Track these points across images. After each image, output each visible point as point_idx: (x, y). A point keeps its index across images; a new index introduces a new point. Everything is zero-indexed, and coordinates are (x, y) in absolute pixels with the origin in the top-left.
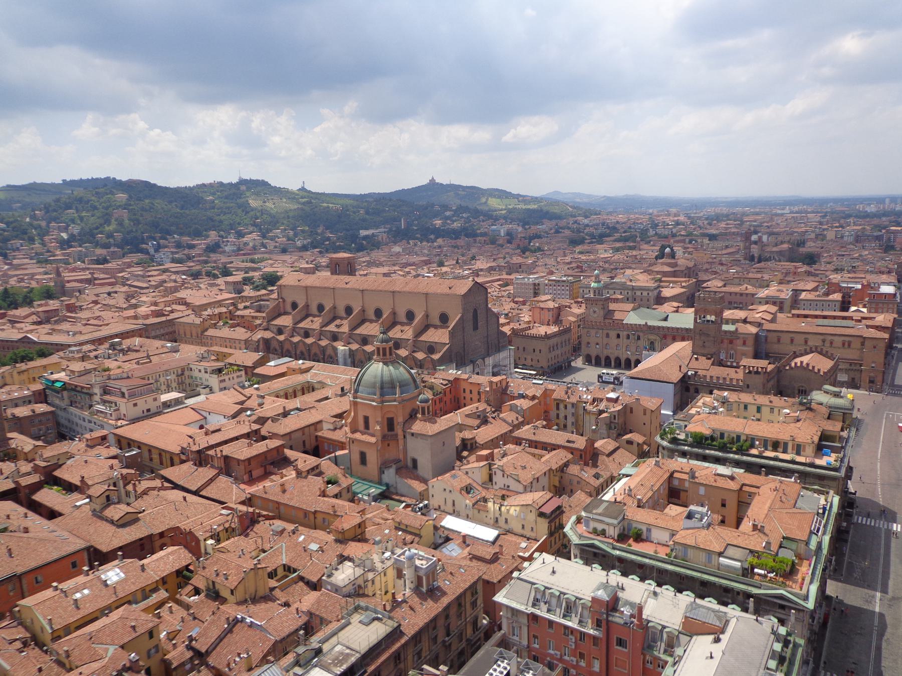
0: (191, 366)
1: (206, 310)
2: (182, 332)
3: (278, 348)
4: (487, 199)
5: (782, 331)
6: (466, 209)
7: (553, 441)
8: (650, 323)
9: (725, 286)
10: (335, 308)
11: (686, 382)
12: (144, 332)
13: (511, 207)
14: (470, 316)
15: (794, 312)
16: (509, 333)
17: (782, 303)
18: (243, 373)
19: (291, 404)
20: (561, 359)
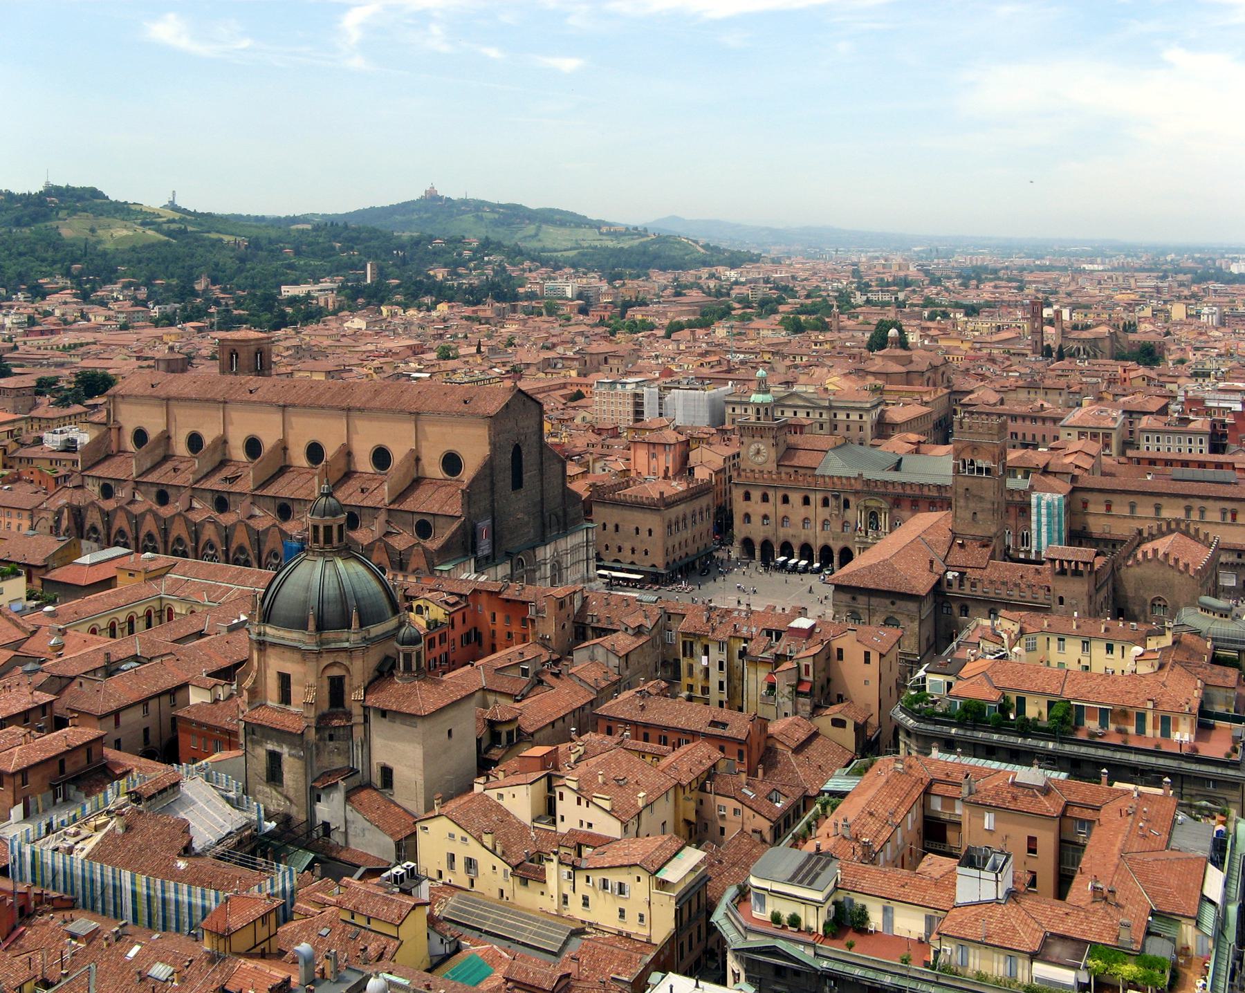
4: (539, 228)
5: (1114, 492)
6: (498, 247)
7: (681, 723)
8: (868, 475)
9: (1002, 402)
10: (225, 442)
11: (943, 594)
13: (585, 244)
14: (506, 460)
15: (1130, 453)
16: (585, 495)
17: (1107, 436)
19: (123, 647)
20: (692, 549)
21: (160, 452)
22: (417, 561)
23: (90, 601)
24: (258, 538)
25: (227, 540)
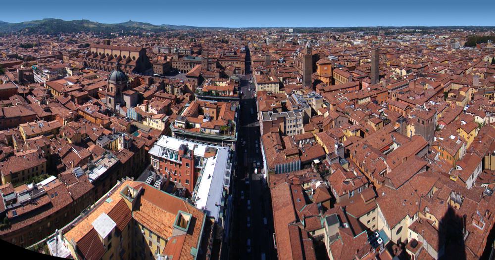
6: (140, 28)
8: (191, 60)
22: (129, 72)
24: (108, 68)
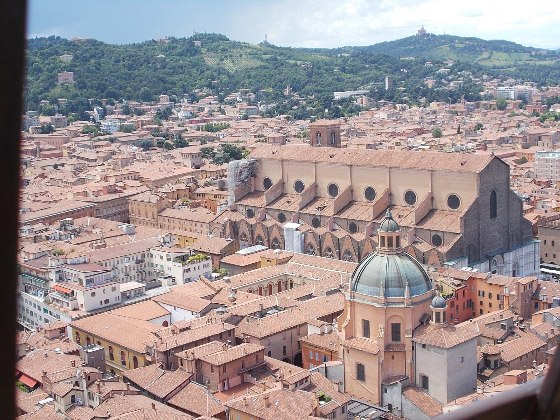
0: (152, 251)
1: (162, 186)
2: (136, 212)
3: (247, 233)
10: (317, 186)
12: (93, 211)
16: (534, 222)
18: (210, 261)
19: (268, 301)
21: (279, 192)
22: (433, 259)
23: (248, 275)
24: (338, 243)
25: (320, 243)
